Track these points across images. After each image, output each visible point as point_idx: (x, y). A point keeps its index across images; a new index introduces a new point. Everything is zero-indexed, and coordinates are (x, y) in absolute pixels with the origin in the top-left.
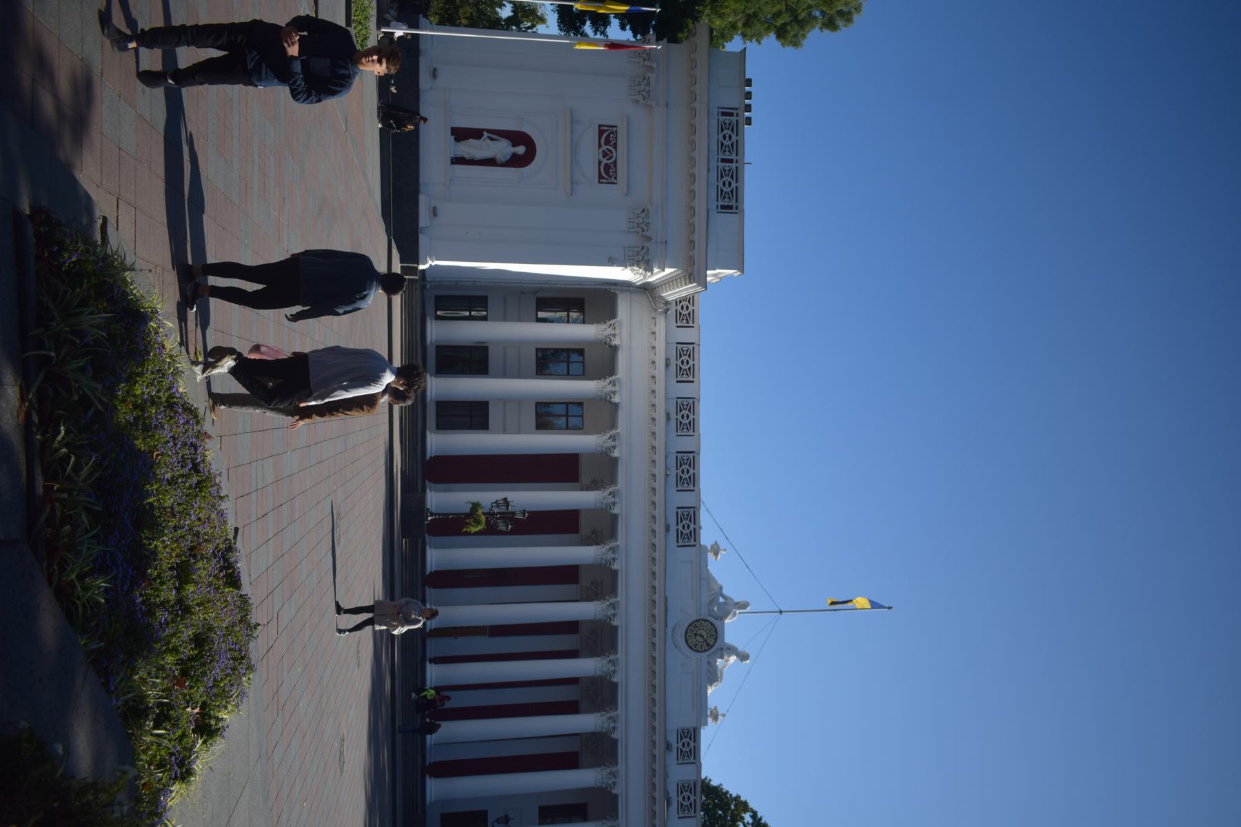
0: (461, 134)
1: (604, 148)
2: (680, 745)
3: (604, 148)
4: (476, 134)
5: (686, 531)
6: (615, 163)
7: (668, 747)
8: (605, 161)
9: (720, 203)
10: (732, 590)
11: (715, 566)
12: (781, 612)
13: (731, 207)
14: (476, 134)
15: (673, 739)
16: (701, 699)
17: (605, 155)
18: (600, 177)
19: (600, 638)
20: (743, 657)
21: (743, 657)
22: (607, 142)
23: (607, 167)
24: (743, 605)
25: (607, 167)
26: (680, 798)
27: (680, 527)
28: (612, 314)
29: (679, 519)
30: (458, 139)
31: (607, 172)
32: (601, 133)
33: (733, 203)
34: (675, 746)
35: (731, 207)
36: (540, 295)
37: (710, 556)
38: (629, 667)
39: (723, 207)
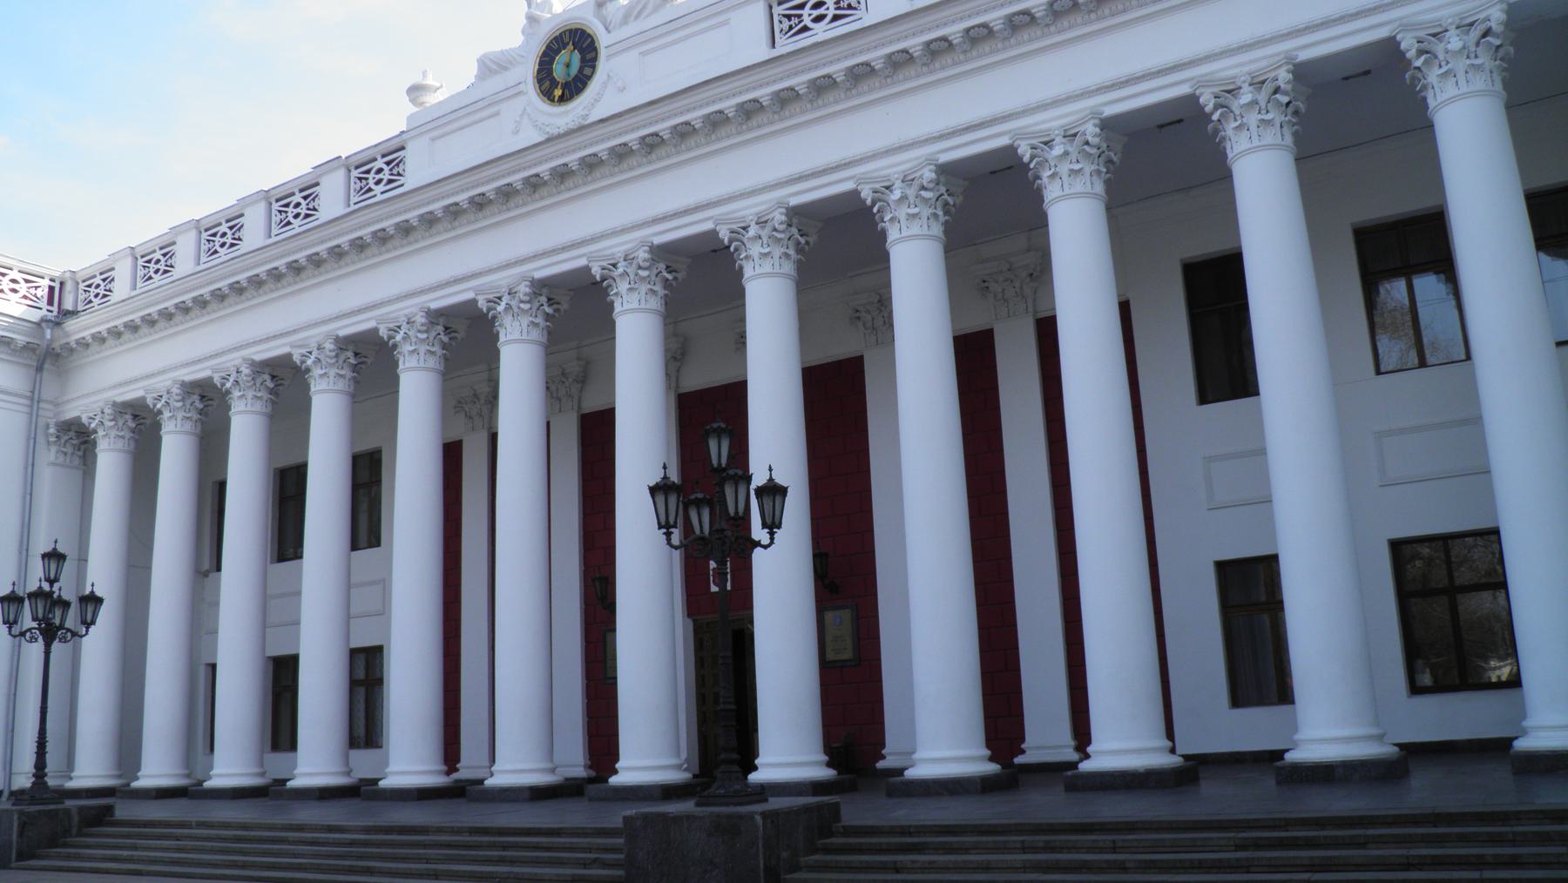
27: (381, 187)
37: (432, 99)
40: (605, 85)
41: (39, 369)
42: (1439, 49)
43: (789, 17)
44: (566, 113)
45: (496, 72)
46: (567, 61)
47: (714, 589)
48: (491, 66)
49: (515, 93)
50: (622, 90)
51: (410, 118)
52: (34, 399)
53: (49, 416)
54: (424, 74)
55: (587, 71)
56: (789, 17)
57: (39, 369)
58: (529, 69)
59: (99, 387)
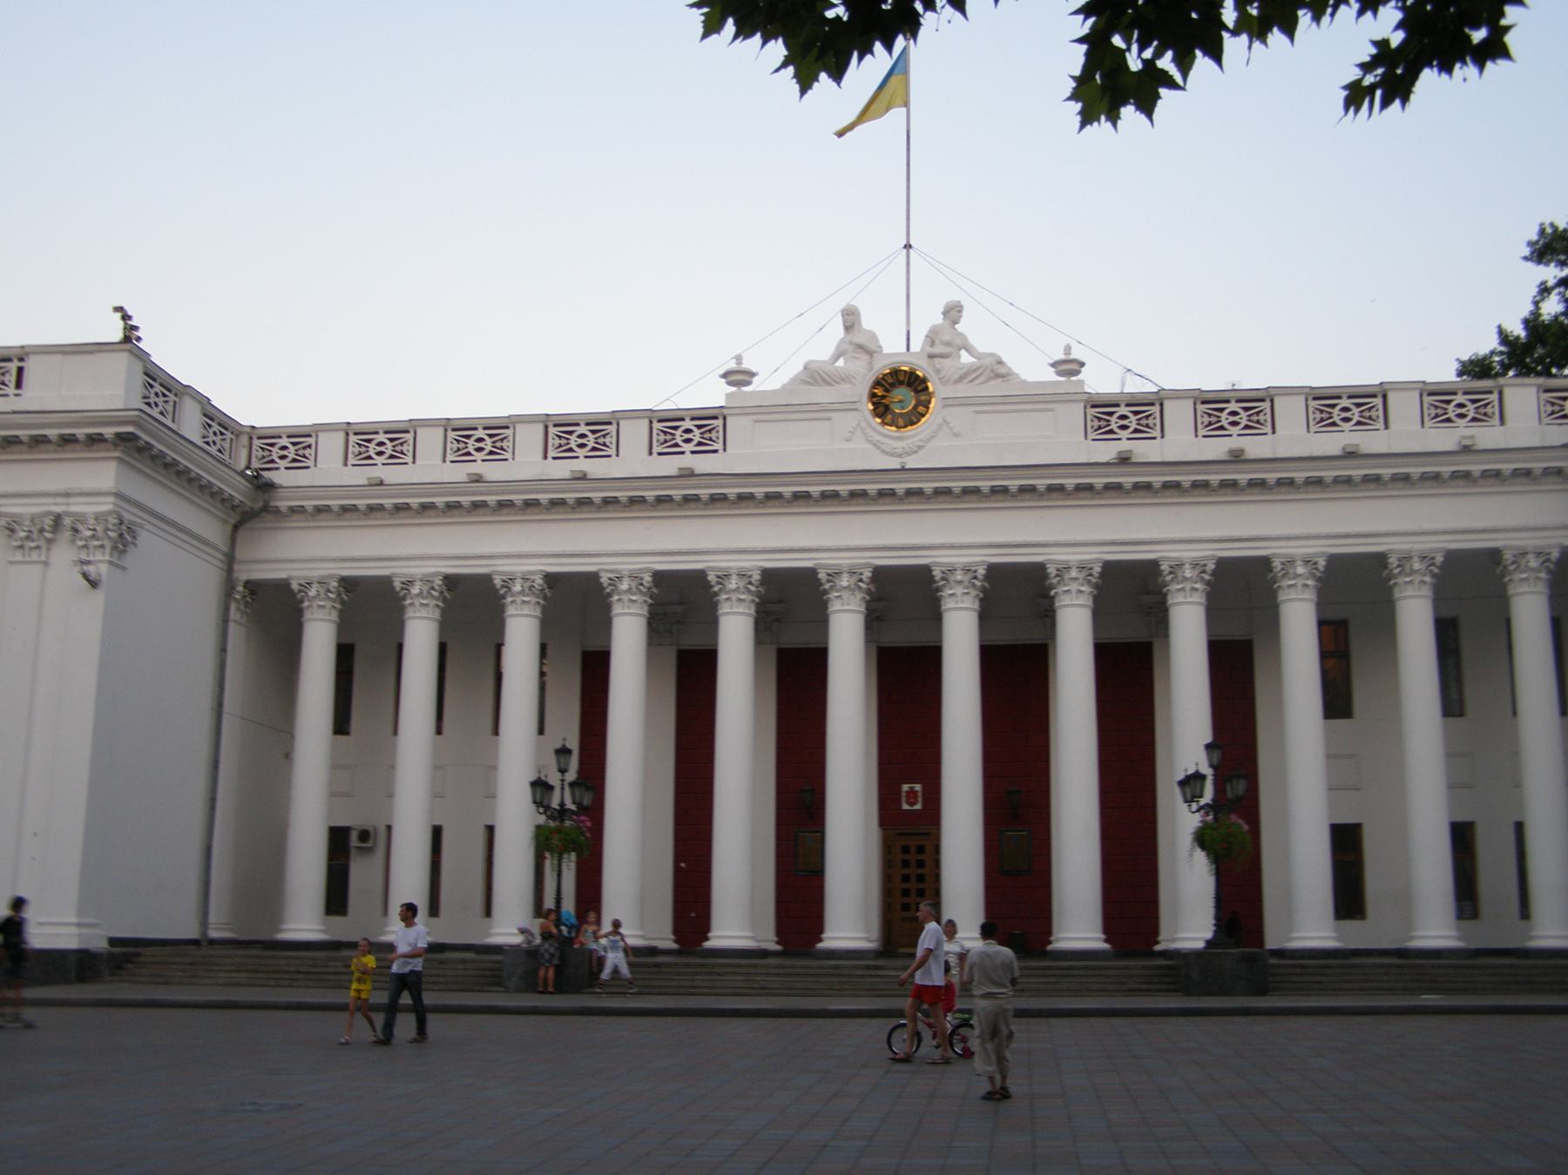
2: (1125, 434)
5: (696, 436)
7: (1124, 460)
9: (11, 390)
10: (822, 343)
11: (771, 379)
12: (908, 246)
13: (20, 370)
15: (1106, 452)
16: (1038, 399)
19: (903, 597)
20: (953, 312)
21: (953, 312)
24: (851, 319)
26: (1235, 430)
28: (283, 586)
29: (673, 450)
33: (13, 366)
34: (1124, 445)
35: (20, 370)
38: (958, 542)
39: (19, 385)
40: (940, 426)
41: (236, 528)
42: (1523, 562)
43: (1099, 419)
44: (899, 438)
45: (828, 384)
46: (899, 393)
47: (905, 807)
48: (814, 375)
49: (850, 407)
50: (956, 435)
51: (728, 396)
52: (230, 560)
53: (244, 574)
54: (739, 359)
55: (921, 409)
56: (1099, 419)
57: (236, 528)
58: (862, 389)
59: (307, 556)
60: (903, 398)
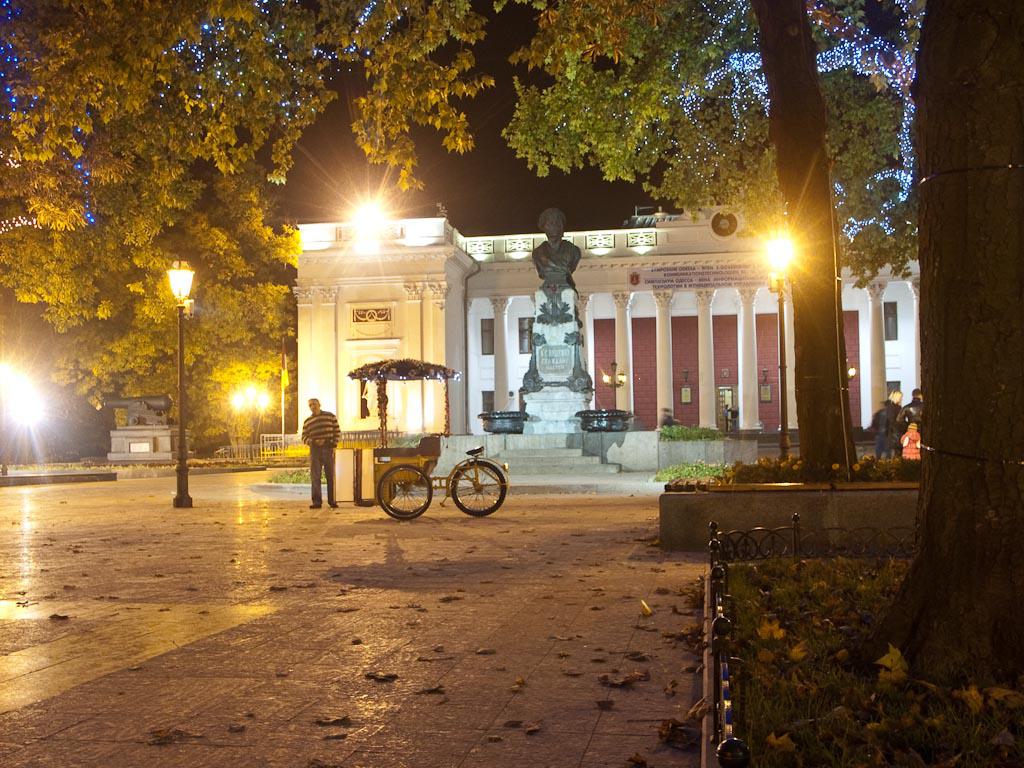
0: (365, 413)
1: (367, 318)
3: (367, 318)
4: (364, 402)
6: (377, 310)
8: (376, 318)
14: (364, 402)
17: (372, 317)
18: (386, 320)
22: (363, 316)
23: (379, 316)
25: (379, 316)
30: (368, 415)
31: (384, 315)
32: (358, 320)
36: (481, 353)
60: (724, 224)
